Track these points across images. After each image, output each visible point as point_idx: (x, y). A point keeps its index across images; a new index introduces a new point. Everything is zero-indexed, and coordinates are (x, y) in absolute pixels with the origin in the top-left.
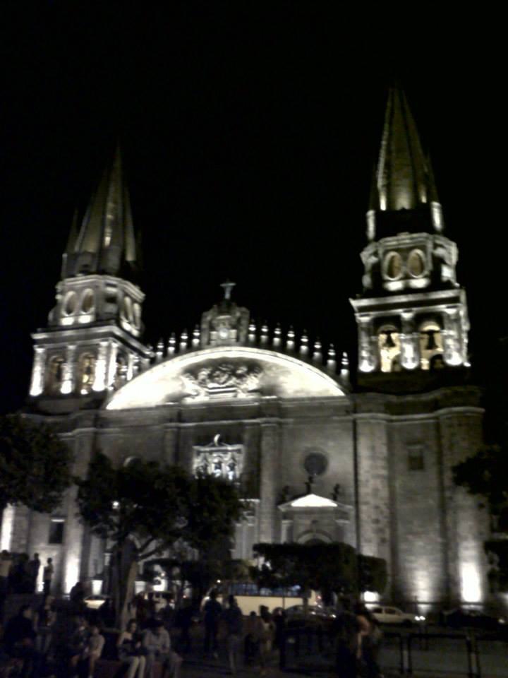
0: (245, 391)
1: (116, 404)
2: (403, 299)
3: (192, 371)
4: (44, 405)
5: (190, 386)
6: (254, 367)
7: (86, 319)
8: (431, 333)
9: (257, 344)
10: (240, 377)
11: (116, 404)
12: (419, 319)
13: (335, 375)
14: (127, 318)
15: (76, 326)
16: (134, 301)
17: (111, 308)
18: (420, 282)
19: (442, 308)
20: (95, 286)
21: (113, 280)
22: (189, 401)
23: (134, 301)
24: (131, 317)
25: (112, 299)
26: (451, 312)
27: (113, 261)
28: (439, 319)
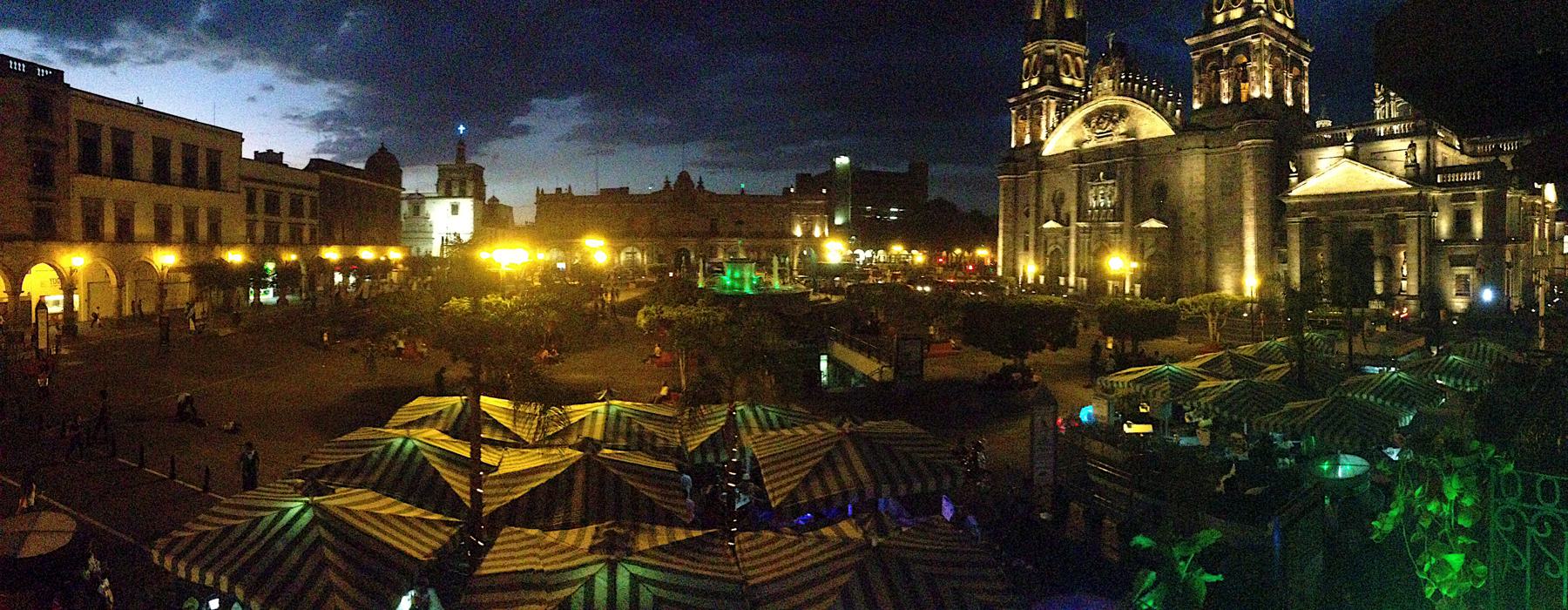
0: (1116, 136)
1: (1048, 151)
2: (1221, 33)
3: (1087, 120)
4: (1018, 155)
5: (1086, 133)
6: (1123, 112)
7: (1035, 82)
8: (1244, 65)
9: (1123, 93)
10: (1115, 122)
11: (1048, 151)
12: (1232, 53)
13: (1169, 119)
14: (1067, 72)
15: (1031, 88)
16: (1074, 55)
17: (1050, 68)
18: (1237, 13)
19: (1248, 38)
20: (1038, 52)
21: (1051, 42)
22: (1086, 146)
23: (1074, 55)
24: (1073, 71)
25: (1051, 60)
26: (1255, 41)
27: (1051, 24)
28: (1246, 49)
